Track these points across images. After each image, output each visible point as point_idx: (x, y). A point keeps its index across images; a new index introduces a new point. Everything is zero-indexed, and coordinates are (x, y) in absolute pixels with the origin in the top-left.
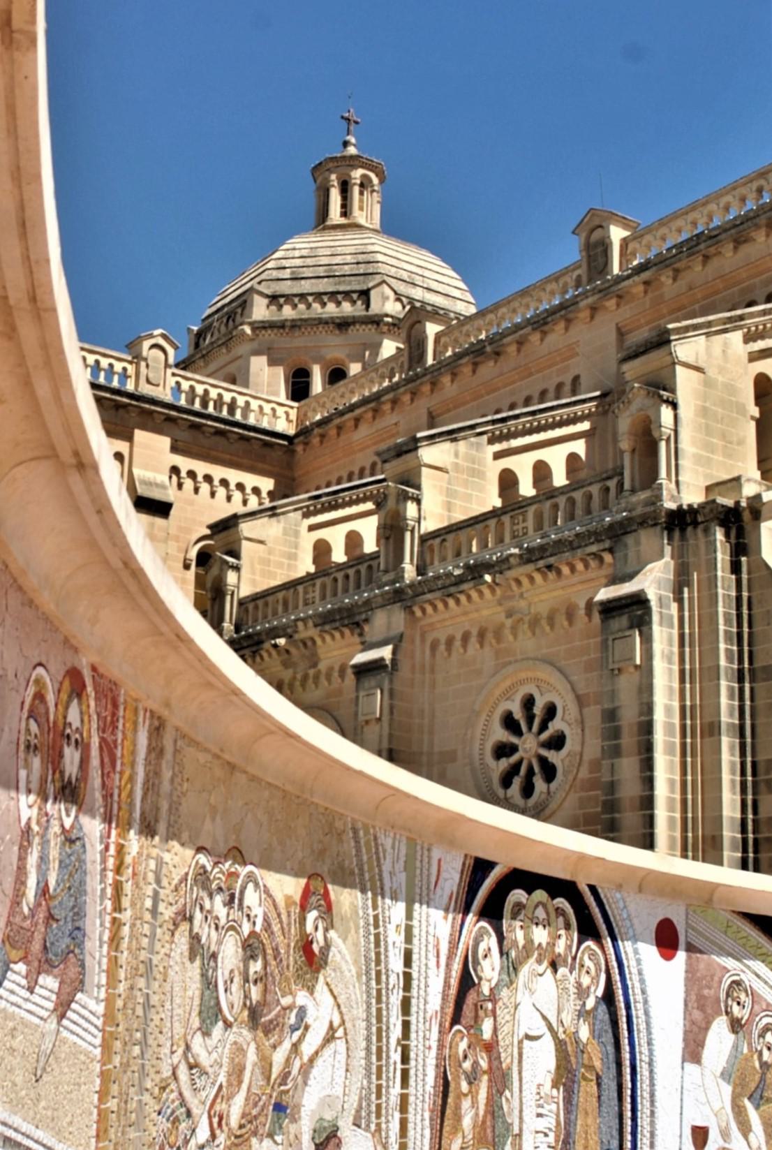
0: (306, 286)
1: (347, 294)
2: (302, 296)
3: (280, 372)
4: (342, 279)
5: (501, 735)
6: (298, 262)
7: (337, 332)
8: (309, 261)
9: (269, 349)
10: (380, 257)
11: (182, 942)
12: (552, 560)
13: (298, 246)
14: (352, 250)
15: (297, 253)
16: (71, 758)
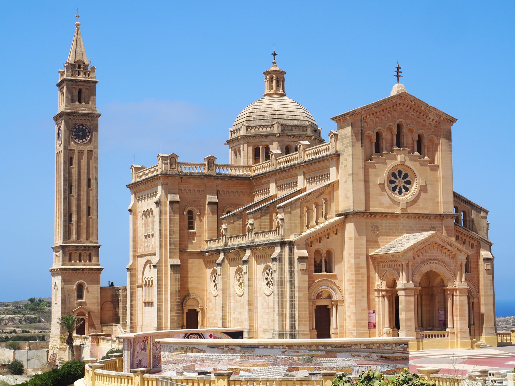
0: (258, 123)
1: (268, 126)
2: (256, 127)
3: (250, 148)
4: (267, 120)
5: (266, 275)
6: (255, 114)
7: (265, 138)
8: (258, 114)
9: (248, 143)
10: (277, 112)
11: (154, 346)
12: (268, 246)
13: (257, 107)
14: (270, 109)
15: (255, 110)
16: (144, 341)
